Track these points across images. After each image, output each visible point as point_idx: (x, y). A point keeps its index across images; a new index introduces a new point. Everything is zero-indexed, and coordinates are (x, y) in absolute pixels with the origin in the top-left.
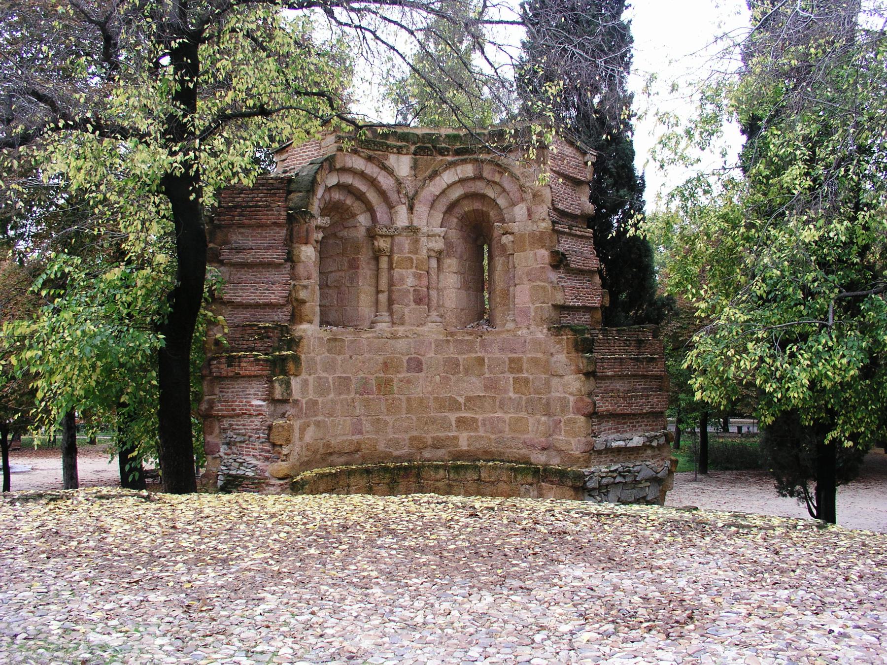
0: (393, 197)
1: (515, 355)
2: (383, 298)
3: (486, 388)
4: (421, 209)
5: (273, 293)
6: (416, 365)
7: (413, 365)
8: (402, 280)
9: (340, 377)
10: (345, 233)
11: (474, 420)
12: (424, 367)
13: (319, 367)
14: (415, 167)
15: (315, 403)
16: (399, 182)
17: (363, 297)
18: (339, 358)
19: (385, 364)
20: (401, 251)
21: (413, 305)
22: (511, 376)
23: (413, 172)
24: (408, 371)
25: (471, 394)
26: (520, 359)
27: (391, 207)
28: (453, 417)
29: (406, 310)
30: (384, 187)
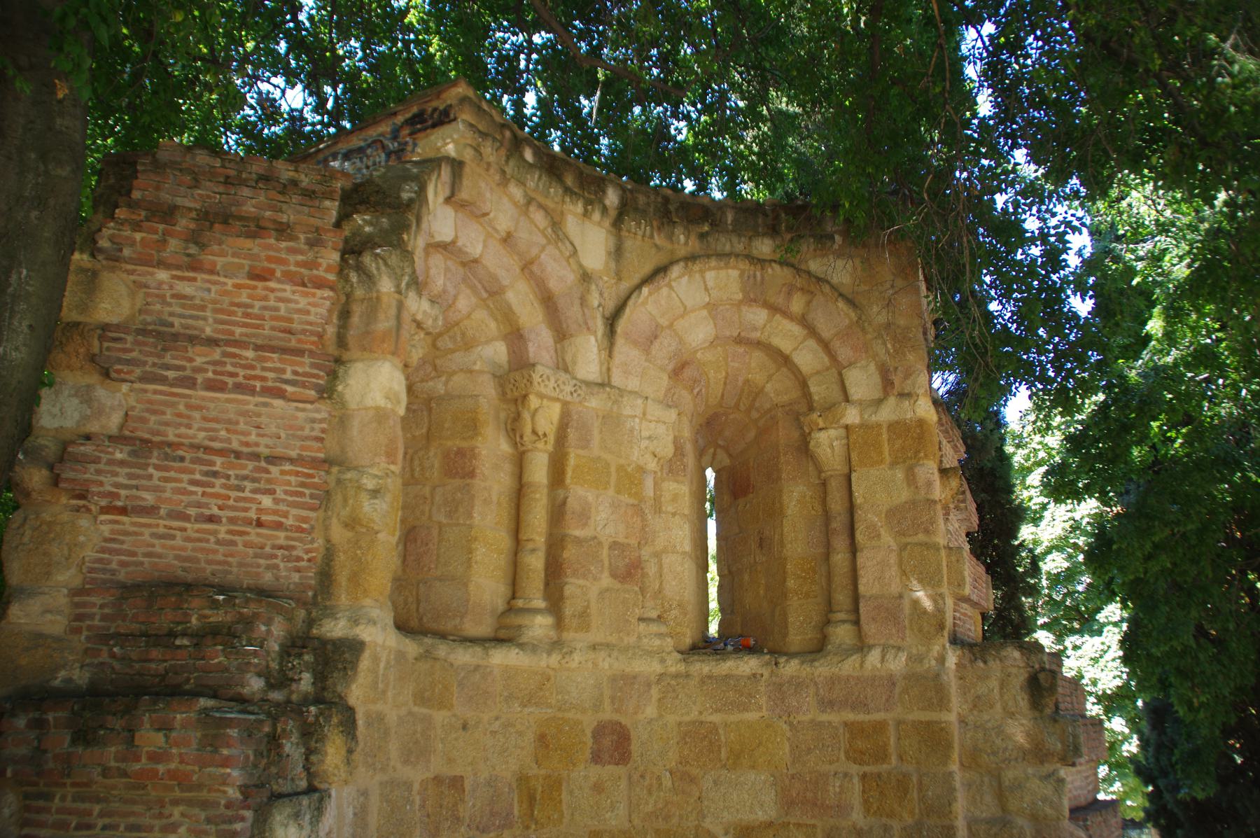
0: (572, 312)
1: (861, 717)
3: (788, 803)
5: (271, 492)
6: (614, 744)
7: (607, 742)
9: (438, 780)
10: (439, 387)
12: (635, 747)
13: (394, 748)
14: (618, 252)
16: (586, 277)
17: (480, 552)
18: (440, 716)
19: (542, 738)
20: (585, 443)
21: (606, 581)
22: (854, 769)
23: (613, 265)
24: (597, 758)
25: (747, 817)
26: (880, 727)
27: (562, 336)
29: (593, 594)
30: (553, 284)
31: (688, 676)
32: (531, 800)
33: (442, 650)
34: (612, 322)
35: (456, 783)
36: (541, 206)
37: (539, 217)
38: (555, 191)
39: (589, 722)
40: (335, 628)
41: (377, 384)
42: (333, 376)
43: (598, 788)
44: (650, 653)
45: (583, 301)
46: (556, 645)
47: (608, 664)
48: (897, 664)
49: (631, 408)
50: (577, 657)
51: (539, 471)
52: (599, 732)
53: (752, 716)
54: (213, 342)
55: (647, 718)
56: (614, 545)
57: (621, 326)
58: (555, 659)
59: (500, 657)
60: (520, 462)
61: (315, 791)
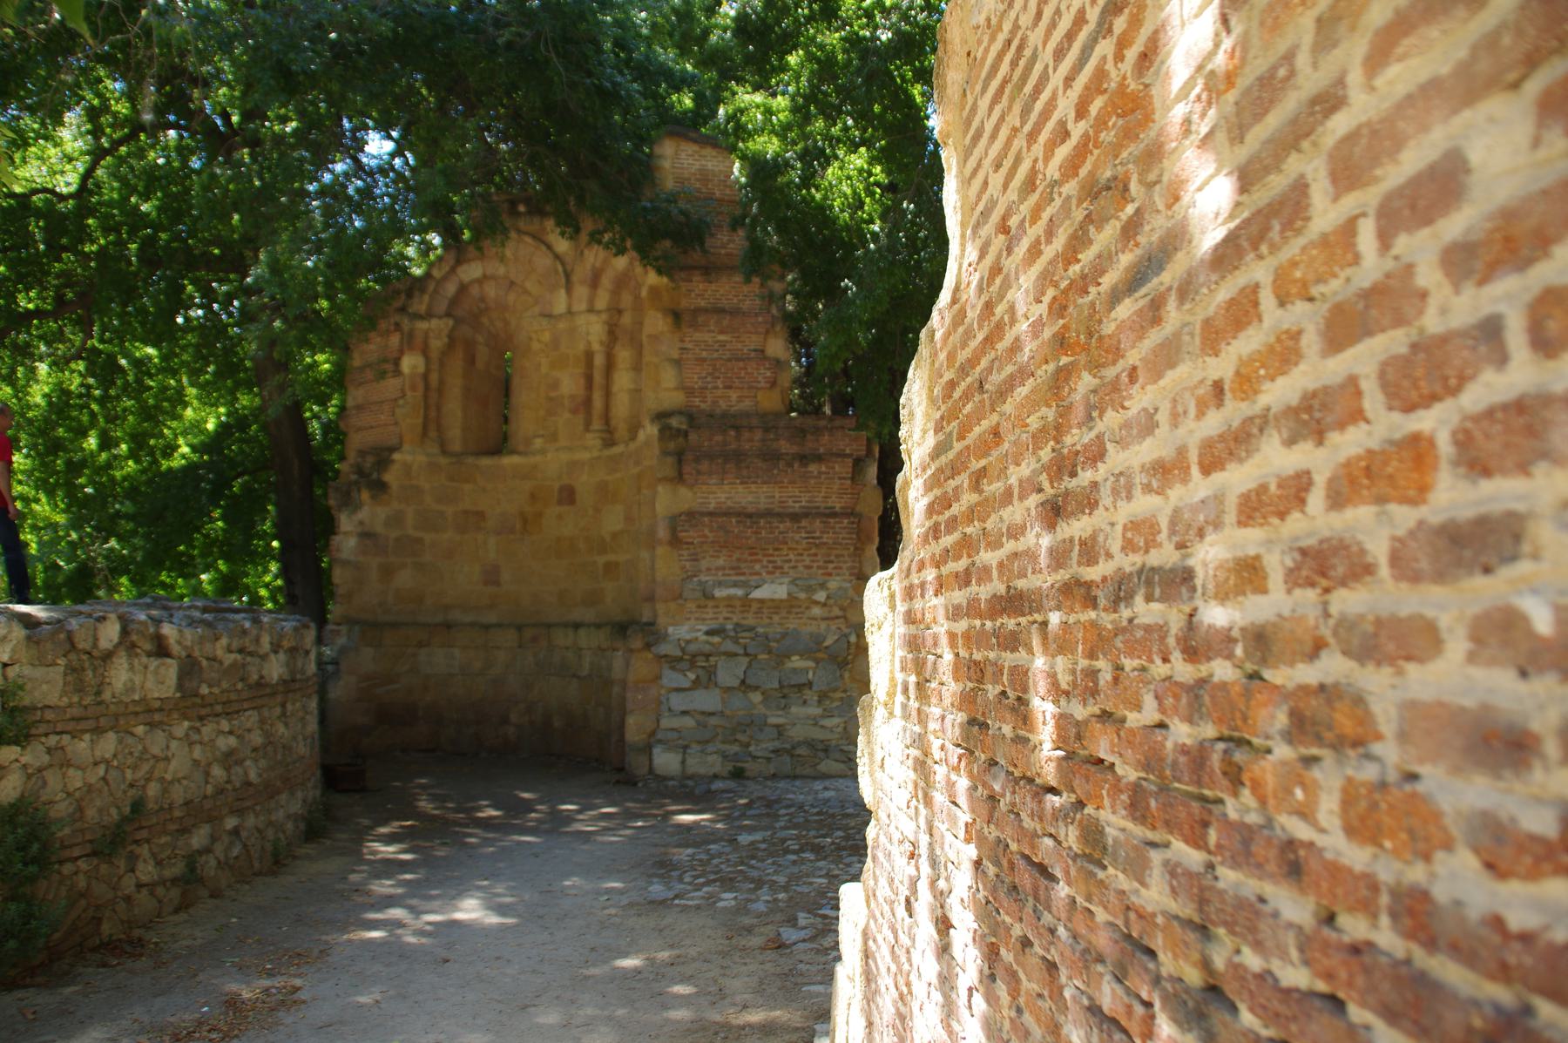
4: (581, 291)
6: (568, 495)
8: (555, 385)
9: (466, 512)
11: (617, 564)
15: (419, 541)
18: (467, 487)
21: (567, 415)
24: (560, 503)
28: (601, 560)
31: (599, 458)
32: (525, 521)
34: (568, 276)
35: (481, 515)
36: (527, 233)
37: (528, 239)
38: (536, 220)
39: (557, 485)
43: (560, 517)
44: (586, 448)
45: (556, 272)
47: (565, 457)
49: (581, 321)
50: (549, 456)
52: (562, 489)
53: (618, 475)
55: (584, 483)
56: (572, 397)
57: (575, 278)
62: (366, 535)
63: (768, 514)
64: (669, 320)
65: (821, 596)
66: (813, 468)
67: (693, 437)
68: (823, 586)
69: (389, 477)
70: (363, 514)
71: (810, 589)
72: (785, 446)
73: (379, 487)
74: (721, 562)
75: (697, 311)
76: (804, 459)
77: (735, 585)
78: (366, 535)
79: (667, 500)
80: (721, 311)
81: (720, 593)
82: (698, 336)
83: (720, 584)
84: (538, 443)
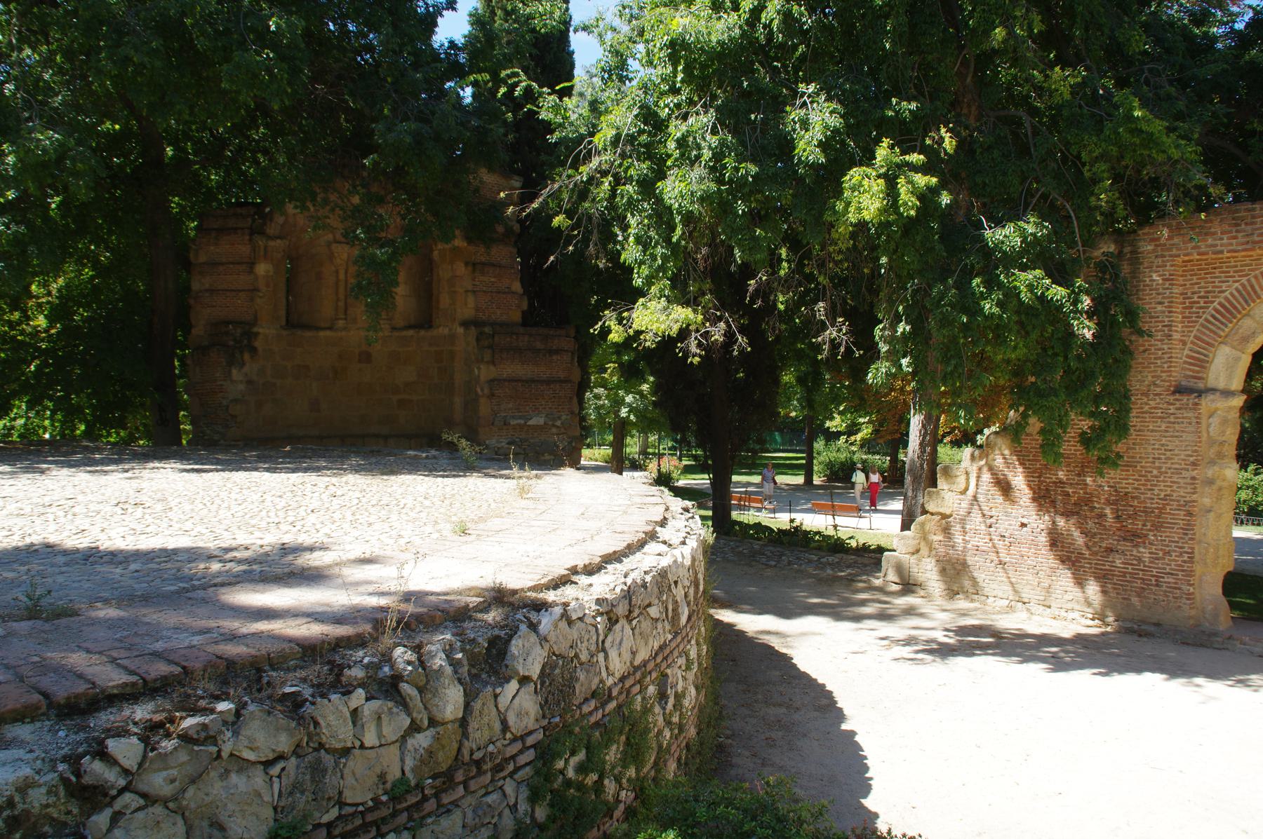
2: (341, 304)
6: (366, 357)
24: (360, 361)
33: (299, 332)
40: (255, 330)
41: (262, 269)
42: (252, 268)
46: (345, 329)
48: (446, 331)
51: (342, 276)
54: (222, 264)
58: (344, 333)
59: (328, 333)
60: (337, 272)
61: (243, 364)
62: (250, 382)
63: (533, 381)
64: (470, 268)
65: (558, 423)
66: (555, 357)
67: (496, 339)
68: (559, 418)
69: (258, 344)
70: (246, 369)
71: (554, 420)
72: (539, 345)
73: (254, 350)
74: (510, 405)
75: (483, 264)
76: (551, 352)
77: (520, 418)
78: (250, 382)
79: (485, 372)
80: (494, 265)
81: (513, 422)
82: (482, 278)
83: (513, 417)
84: (341, 323)
